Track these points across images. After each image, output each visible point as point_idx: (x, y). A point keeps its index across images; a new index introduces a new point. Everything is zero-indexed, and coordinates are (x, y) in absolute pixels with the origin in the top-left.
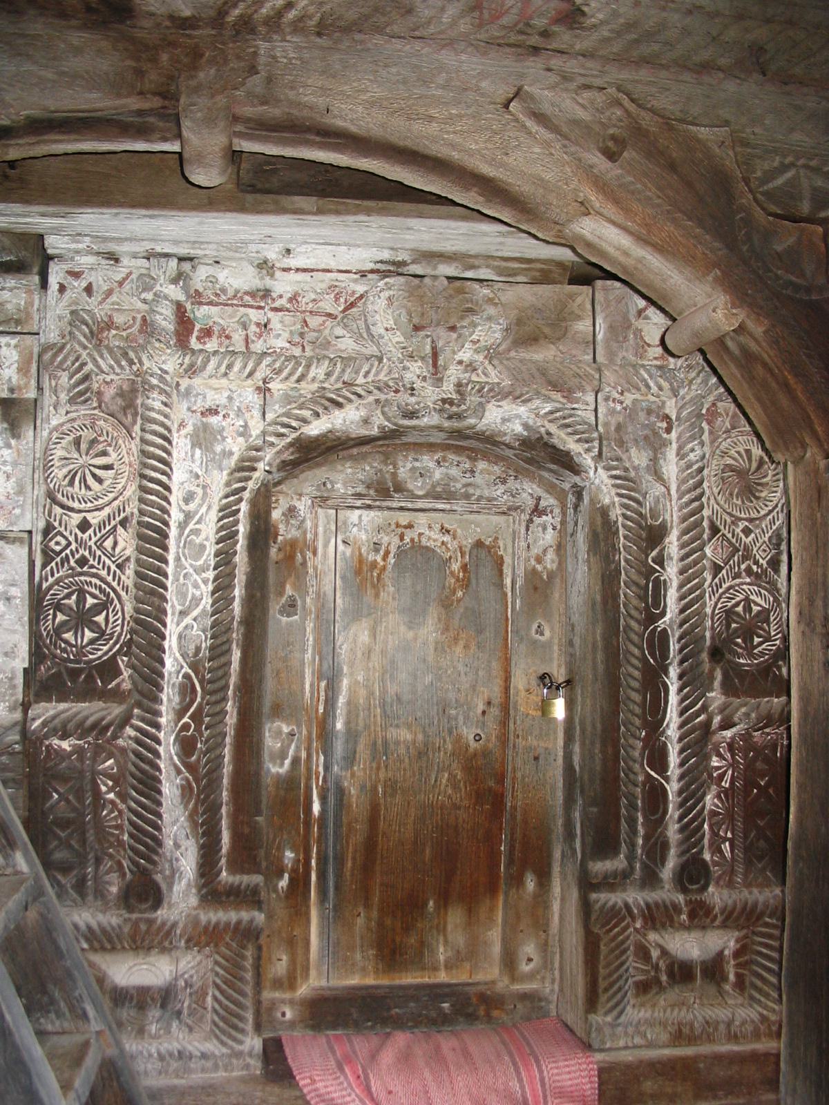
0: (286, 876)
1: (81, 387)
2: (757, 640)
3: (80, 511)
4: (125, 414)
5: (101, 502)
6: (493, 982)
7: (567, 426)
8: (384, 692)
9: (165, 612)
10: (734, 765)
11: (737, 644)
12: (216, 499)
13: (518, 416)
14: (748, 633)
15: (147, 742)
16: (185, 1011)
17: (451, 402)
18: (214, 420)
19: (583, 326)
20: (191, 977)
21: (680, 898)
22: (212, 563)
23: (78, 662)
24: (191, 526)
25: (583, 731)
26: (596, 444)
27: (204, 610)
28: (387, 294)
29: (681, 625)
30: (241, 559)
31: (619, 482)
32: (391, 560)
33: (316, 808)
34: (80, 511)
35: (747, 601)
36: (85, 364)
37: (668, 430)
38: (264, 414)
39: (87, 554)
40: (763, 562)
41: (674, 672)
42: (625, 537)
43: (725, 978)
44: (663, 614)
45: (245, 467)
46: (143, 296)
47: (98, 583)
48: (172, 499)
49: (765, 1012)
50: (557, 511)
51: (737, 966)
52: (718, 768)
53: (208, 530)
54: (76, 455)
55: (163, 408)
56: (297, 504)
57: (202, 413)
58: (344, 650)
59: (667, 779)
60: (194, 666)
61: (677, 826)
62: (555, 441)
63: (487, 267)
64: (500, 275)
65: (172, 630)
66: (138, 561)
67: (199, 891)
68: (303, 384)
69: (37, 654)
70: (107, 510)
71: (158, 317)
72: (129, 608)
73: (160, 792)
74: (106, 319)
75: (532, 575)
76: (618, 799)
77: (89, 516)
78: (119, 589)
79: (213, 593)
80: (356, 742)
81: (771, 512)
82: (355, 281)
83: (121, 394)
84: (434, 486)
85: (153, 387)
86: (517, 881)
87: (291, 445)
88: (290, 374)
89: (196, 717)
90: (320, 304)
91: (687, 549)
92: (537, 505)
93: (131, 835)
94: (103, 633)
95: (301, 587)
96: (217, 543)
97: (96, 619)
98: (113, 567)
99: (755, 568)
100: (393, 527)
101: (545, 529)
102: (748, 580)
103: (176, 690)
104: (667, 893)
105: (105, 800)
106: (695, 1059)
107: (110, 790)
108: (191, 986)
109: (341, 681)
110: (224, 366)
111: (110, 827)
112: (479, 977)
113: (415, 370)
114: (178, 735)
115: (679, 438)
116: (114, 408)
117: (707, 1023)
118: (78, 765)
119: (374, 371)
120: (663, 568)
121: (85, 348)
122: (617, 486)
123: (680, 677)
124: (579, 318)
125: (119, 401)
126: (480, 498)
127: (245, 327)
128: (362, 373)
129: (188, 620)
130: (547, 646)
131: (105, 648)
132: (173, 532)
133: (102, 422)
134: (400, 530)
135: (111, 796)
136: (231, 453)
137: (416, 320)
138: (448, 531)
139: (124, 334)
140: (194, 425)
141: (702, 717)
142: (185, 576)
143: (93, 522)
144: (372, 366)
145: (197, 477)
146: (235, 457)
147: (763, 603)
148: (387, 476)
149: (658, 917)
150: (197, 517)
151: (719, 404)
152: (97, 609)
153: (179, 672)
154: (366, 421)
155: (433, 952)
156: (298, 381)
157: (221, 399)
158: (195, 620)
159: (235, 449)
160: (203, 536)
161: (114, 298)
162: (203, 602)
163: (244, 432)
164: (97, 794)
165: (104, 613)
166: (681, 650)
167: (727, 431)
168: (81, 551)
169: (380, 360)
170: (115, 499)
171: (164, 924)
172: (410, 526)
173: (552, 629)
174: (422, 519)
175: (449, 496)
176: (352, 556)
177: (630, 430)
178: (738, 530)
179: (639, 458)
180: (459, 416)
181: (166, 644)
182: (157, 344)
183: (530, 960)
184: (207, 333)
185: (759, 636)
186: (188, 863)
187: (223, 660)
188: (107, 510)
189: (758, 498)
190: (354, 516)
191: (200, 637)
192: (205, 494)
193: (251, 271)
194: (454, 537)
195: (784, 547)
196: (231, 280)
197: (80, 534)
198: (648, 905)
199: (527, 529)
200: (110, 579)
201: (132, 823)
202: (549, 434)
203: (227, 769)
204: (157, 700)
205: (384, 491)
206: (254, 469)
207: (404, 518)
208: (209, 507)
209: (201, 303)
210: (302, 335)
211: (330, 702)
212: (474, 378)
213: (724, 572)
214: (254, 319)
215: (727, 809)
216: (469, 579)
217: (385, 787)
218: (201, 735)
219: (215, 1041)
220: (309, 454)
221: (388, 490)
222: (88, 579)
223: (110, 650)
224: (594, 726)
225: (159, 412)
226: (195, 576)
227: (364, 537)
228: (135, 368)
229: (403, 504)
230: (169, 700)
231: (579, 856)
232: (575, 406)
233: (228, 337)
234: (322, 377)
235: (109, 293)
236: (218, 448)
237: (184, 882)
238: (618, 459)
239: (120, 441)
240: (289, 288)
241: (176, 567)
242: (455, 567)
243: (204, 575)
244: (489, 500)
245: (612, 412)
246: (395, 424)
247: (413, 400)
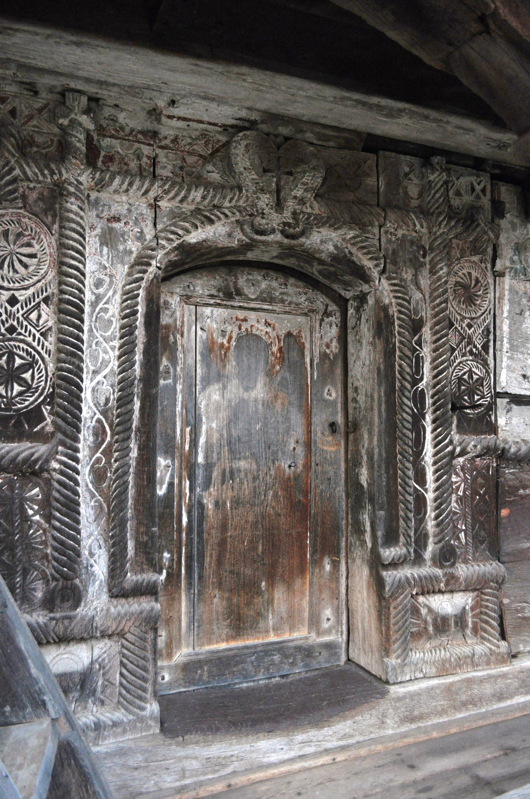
0: (165, 572)
1: (10, 188)
2: (476, 398)
3: (9, 289)
4: (46, 215)
5: (27, 282)
6: (306, 638)
7: (363, 248)
8: (230, 435)
9: (81, 370)
10: (465, 480)
11: (465, 400)
12: (120, 286)
13: (331, 240)
14: (471, 393)
15: (71, 472)
16: (99, 689)
17: (288, 225)
18: (116, 225)
19: (371, 181)
20: (103, 660)
21: (439, 572)
22: (118, 335)
23: (9, 410)
24: (101, 305)
25: (371, 457)
26: (382, 261)
27: (112, 370)
28: (244, 143)
29: (434, 387)
30: (140, 333)
31: (397, 288)
32: (233, 343)
33: (185, 520)
34: (9, 289)
35: (470, 372)
36: (12, 169)
37: (424, 256)
38: (155, 224)
39: (15, 323)
40: (479, 346)
41: (429, 418)
42: (400, 326)
43: (467, 626)
44: (422, 379)
45: (142, 262)
46: (61, 121)
47: (25, 347)
48: (86, 283)
49: (493, 647)
50: (338, 314)
51: (474, 616)
52: (456, 482)
53: (114, 309)
54: (6, 244)
55: (79, 211)
56: (170, 300)
57: (108, 220)
58: (202, 404)
59: (426, 491)
60: (104, 413)
61: (433, 523)
62: (355, 259)
63: (312, 132)
64: (319, 139)
65: (87, 384)
66: (61, 331)
67: (110, 591)
68: (185, 205)
70: (31, 291)
71: (73, 139)
72: (51, 367)
73: (79, 514)
74: (28, 138)
75: (324, 356)
76: (397, 505)
77: (17, 294)
78: (43, 352)
79: (119, 357)
80: (211, 472)
81: (483, 314)
82: (219, 133)
83: (41, 198)
84: (262, 293)
85: (70, 194)
86: (317, 563)
87: (176, 248)
88: (176, 195)
89: (107, 453)
90: (195, 147)
91: (439, 335)
92: (326, 310)
93: (55, 549)
94: (29, 387)
95: (174, 360)
96: (123, 319)
97: (24, 376)
98: (38, 335)
99: (474, 350)
100: (234, 320)
101: (331, 326)
102: (471, 358)
103: (91, 432)
104: (427, 570)
105: (32, 521)
106: (452, 684)
107: (36, 513)
108: (104, 668)
109: (201, 427)
110: (126, 183)
111: (36, 543)
112: (296, 635)
113: (265, 201)
114: (92, 467)
115: (430, 262)
116: (36, 209)
117: (459, 658)
118: (8, 493)
119: (236, 197)
120: (421, 348)
121: (14, 156)
122: (396, 291)
123: (434, 421)
124: (368, 175)
125: (41, 204)
126: (290, 303)
127: (139, 158)
128: (228, 199)
129: (99, 377)
130: (333, 403)
131: (31, 399)
132: (87, 309)
133: (26, 220)
134: (238, 323)
135: (37, 518)
136: (131, 252)
137: (265, 164)
138: (270, 325)
139: (44, 151)
140: (102, 228)
141: (450, 448)
142: (97, 343)
143: (21, 298)
144: (235, 194)
145: (105, 268)
146: (134, 255)
147: (479, 373)
148: (231, 283)
149: (428, 587)
150: (104, 300)
151: (454, 241)
152: (25, 368)
153: (92, 418)
154: (230, 235)
155: (266, 618)
156: (181, 201)
157: (123, 210)
158: (105, 377)
159: (134, 249)
160: (110, 313)
161: (35, 122)
162: (111, 365)
163: (141, 237)
164: (26, 518)
165: (31, 371)
166: (434, 404)
167: (458, 259)
168: (10, 322)
169: (240, 191)
170: (39, 281)
171: (83, 619)
172: (245, 320)
173: (337, 392)
174: (252, 315)
175: (271, 300)
176: (207, 339)
177: (401, 254)
178: (464, 325)
179: (408, 275)
180: (293, 237)
181: (83, 395)
182: (74, 161)
183: (328, 619)
184: (110, 159)
185: (478, 395)
186: (100, 567)
187: (129, 407)
188: (31, 291)
189: (475, 305)
190: (208, 311)
192: (111, 282)
193: (143, 115)
194: (274, 329)
195: (491, 337)
196: (127, 121)
197: (9, 308)
198: (419, 577)
199: (321, 326)
200: (35, 344)
201: (55, 538)
202: (350, 253)
203: (131, 492)
204: (76, 440)
205: (228, 295)
206: (150, 265)
207: (241, 314)
208: (115, 292)
209: (105, 136)
210: (181, 168)
211: (194, 443)
212: (305, 210)
213: (456, 352)
214: (146, 153)
215: (461, 510)
216: (283, 358)
217: (232, 502)
218: (111, 466)
219: (123, 710)
221: (231, 293)
222: (17, 344)
223: (36, 400)
224: (380, 454)
225: (76, 214)
226: (105, 344)
227: (215, 326)
228: (56, 178)
229: (241, 304)
230: (85, 439)
231: (369, 545)
232: (367, 235)
233: (126, 164)
234: (198, 199)
235: (30, 117)
236: (121, 248)
237: (97, 583)
238: (396, 273)
239: (42, 236)
240: (172, 132)
241: (90, 336)
242: (275, 349)
243: (111, 343)
244: (297, 304)
245: (389, 241)
246: (251, 239)
247: (264, 221)
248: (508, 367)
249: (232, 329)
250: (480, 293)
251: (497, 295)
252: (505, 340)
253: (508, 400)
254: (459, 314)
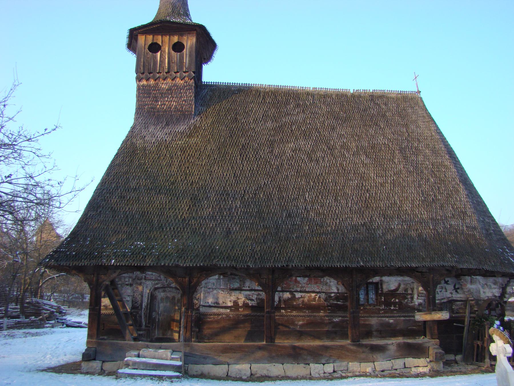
53: (147, 295)
69: (132, 306)
186: (144, 324)
191: (146, 304)
205: (164, 291)
220: (156, 289)
249: (165, 296)
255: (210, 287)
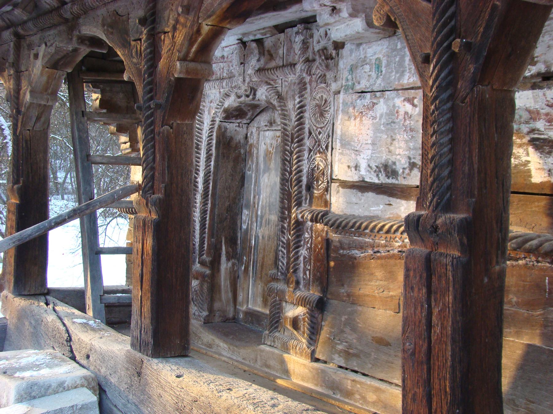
52: (307, 238)
195: (330, 140)
215: (309, 256)
248: (340, 160)
250: (328, 108)
251: (336, 108)
252: (338, 141)
253: (337, 184)
254: (315, 126)
255: (363, 85)
